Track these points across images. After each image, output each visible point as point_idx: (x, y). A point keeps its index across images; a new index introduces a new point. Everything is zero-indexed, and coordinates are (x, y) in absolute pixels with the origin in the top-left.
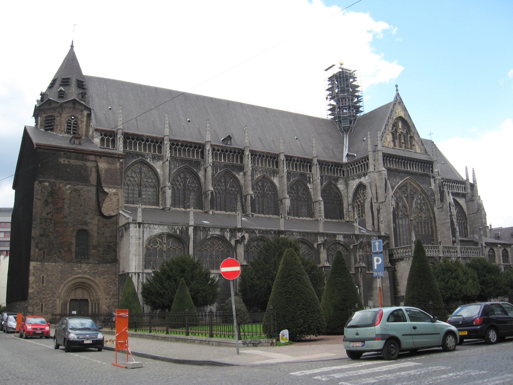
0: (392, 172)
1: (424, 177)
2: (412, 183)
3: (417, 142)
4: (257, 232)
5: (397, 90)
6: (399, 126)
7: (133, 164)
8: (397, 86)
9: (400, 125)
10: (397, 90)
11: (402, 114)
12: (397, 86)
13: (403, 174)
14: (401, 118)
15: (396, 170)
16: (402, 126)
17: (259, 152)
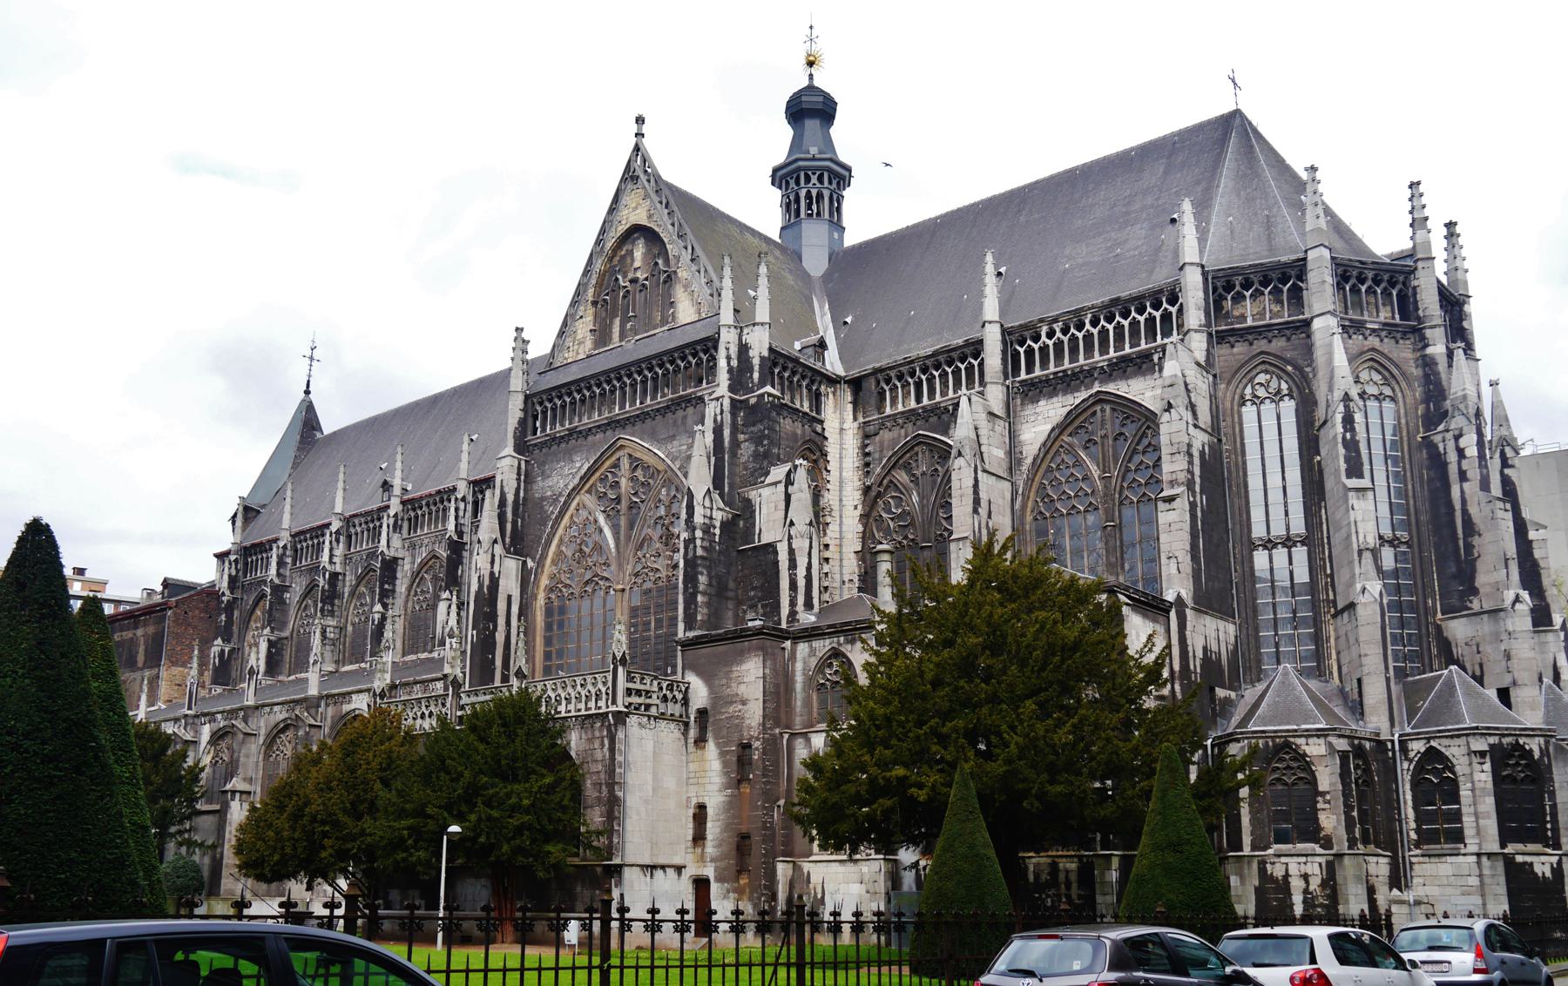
0: (563, 445)
1: (680, 413)
2: (638, 455)
3: (686, 287)
4: (219, 716)
5: (639, 135)
6: (633, 260)
7: (256, 604)
8: (640, 120)
9: (639, 251)
10: (639, 135)
11: (640, 217)
12: (640, 120)
13: (600, 436)
14: (636, 230)
15: (572, 432)
16: (645, 255)
17: (421, 498)
